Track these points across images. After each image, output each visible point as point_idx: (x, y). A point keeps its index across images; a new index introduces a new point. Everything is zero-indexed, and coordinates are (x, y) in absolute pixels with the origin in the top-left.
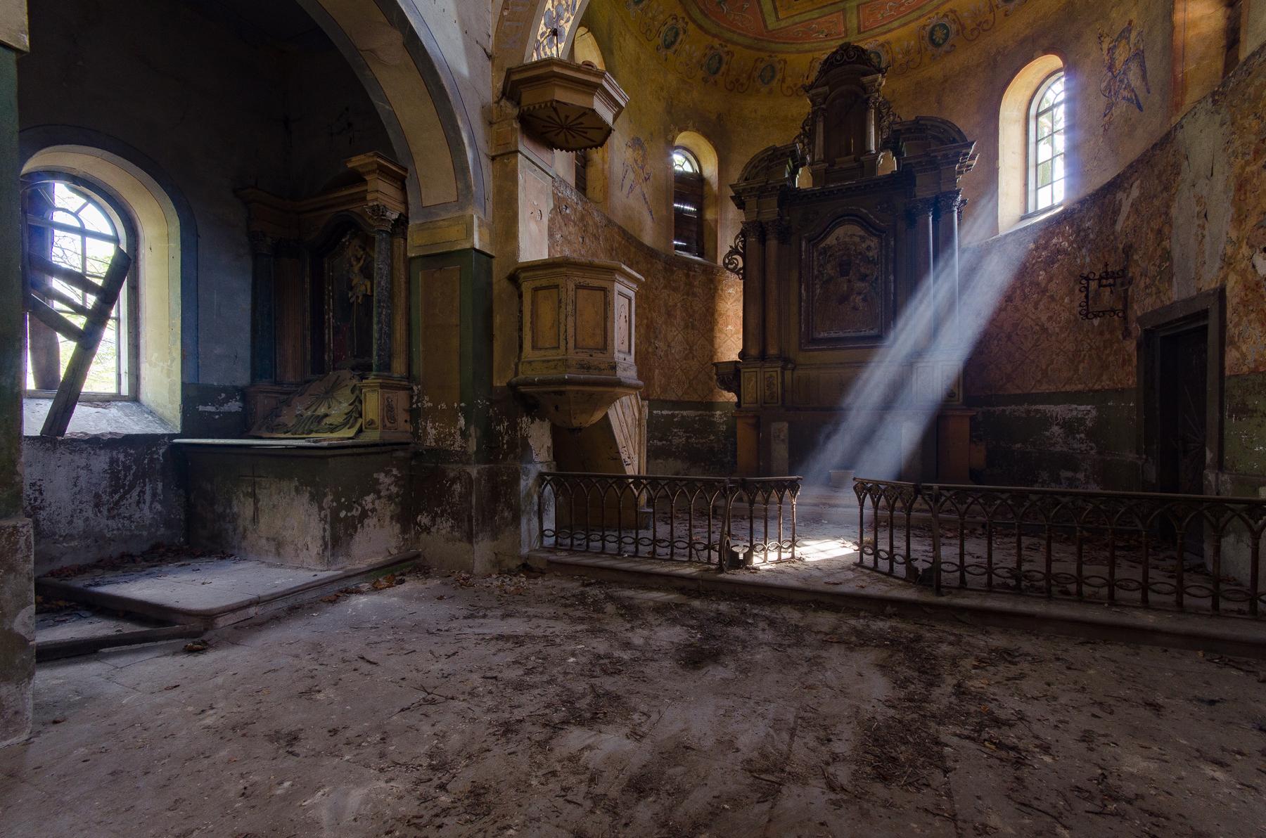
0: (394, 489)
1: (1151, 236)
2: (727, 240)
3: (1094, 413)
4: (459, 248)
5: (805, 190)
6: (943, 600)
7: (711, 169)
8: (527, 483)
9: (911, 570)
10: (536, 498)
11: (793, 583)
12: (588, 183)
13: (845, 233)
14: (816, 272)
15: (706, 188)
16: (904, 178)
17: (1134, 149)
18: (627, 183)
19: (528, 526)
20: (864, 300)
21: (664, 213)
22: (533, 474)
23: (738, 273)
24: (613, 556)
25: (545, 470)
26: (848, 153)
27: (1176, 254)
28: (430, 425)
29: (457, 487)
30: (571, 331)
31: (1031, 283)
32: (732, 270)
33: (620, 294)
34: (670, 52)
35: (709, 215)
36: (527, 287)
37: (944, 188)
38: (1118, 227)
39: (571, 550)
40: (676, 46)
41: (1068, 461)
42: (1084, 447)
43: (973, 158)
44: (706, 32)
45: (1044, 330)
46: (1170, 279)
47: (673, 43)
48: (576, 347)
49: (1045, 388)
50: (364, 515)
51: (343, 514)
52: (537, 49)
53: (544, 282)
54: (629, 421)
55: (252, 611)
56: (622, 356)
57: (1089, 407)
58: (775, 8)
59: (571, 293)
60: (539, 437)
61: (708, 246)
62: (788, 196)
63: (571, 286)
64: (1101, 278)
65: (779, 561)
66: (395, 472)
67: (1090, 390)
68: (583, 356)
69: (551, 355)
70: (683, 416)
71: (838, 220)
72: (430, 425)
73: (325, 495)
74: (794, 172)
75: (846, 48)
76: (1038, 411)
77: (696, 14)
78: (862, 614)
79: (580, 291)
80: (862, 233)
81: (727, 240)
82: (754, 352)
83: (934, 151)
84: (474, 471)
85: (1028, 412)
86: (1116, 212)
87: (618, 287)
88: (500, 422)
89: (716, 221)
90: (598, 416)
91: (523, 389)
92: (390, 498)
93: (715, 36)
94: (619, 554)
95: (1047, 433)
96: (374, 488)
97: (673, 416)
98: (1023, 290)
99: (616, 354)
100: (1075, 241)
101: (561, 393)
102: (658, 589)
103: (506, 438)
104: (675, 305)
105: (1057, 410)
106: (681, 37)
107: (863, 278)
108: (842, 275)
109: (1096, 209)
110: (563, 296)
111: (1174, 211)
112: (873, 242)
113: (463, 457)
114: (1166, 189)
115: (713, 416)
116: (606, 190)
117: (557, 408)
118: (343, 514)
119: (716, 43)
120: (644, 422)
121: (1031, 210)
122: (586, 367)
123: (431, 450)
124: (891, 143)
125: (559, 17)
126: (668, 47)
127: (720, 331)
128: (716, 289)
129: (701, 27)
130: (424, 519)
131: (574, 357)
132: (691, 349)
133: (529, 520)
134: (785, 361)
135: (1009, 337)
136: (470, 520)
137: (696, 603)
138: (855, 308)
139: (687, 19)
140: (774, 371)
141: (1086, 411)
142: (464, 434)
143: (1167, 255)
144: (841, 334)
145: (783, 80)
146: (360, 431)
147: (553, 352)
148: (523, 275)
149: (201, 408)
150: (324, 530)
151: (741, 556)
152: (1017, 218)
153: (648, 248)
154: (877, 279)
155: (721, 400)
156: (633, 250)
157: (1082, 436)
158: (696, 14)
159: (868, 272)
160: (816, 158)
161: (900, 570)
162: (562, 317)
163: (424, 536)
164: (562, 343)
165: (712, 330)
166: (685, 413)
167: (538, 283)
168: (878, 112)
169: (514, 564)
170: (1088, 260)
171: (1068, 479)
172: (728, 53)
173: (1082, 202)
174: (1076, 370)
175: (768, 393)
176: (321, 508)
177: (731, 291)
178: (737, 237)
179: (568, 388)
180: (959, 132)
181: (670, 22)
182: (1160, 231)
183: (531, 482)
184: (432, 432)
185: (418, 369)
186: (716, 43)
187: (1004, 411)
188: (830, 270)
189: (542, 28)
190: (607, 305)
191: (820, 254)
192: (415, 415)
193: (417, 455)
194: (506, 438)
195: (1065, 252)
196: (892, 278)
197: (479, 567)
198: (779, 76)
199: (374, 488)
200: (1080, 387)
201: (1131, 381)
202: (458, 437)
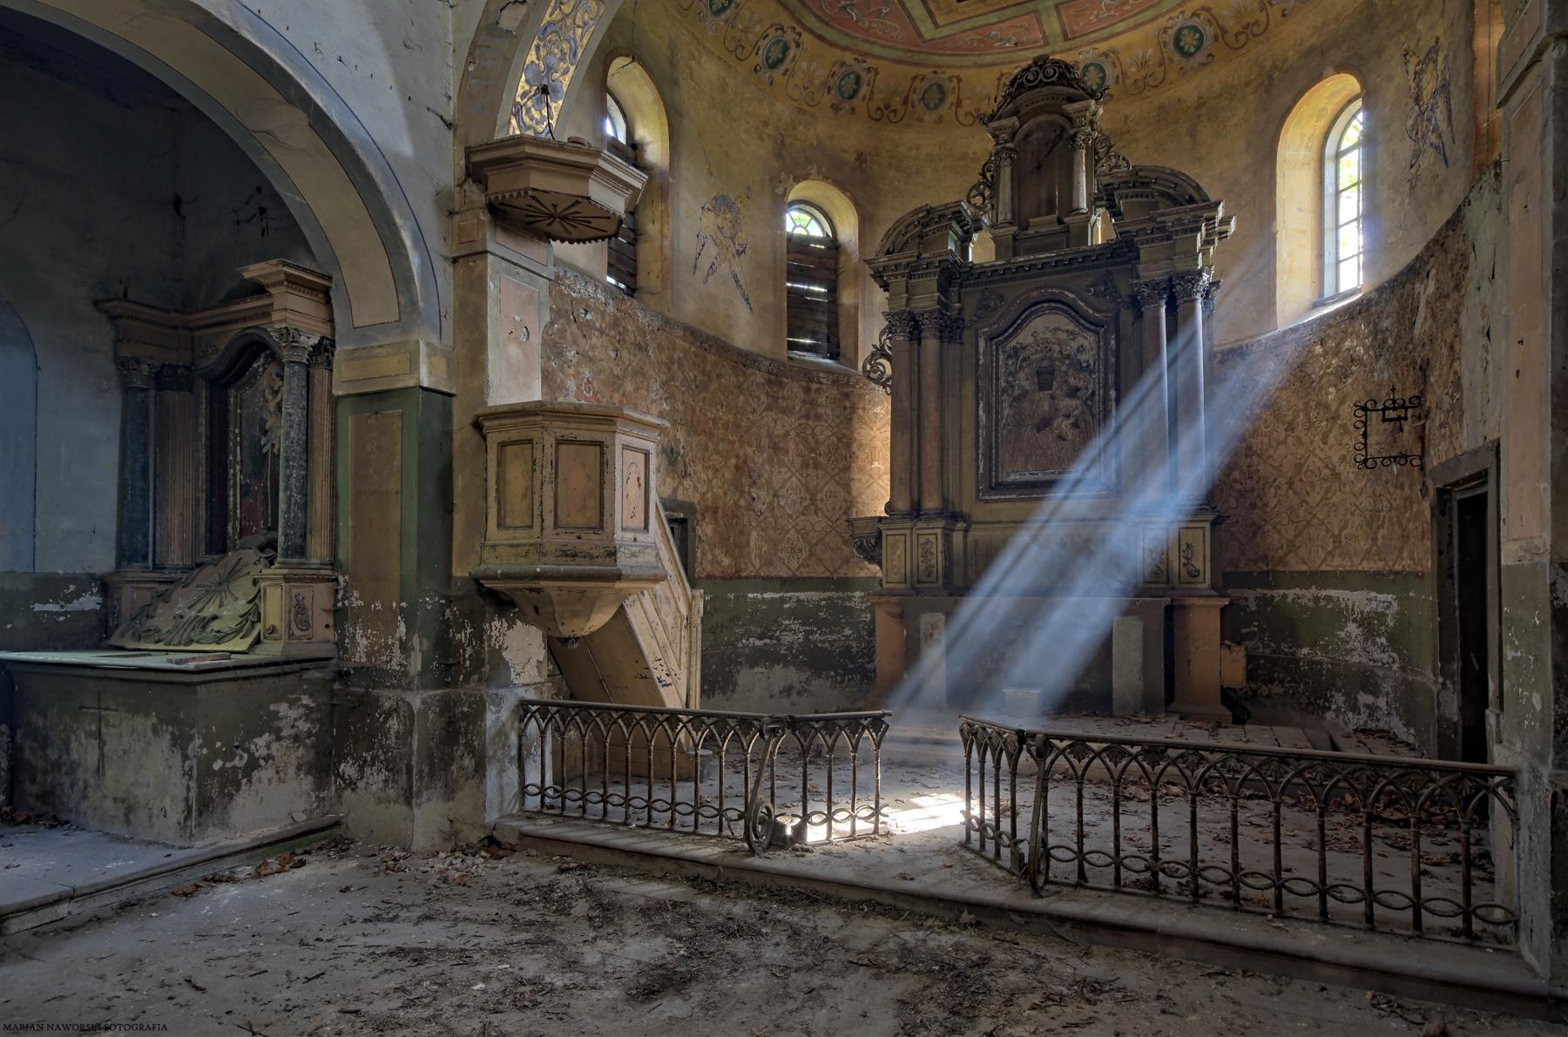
0: (303, 726)
1: (1445, 351)
2: (870, 332)
3: (1395, 606)
4: (400, 385)
5: (981, 266)
6: (1038, 904)
7: (848, 231)
8: (497, 717)
9: (1018, 857)
10: (513, 738)
11: (845, 873)
12: (641, 266)
14: (1003, 384)
15: (842, 259)
16: (1122, 251)
17: (1439, 217)
18: (705, 263)
19: (500, 783)
20: (1075, 425)
21: (771, 299)
22: (510, 699)
24: (615, 826)
25: (531, 695)
26: (1050, 211)
27: (1465, 382)
28: (359, 632)
30: (549, 504)
31: (1318, 404)
32: (877, 381)
33: (626, 447)
34: (777, 74)
35: (847, 298)
36: (493, 439)
37: (1181, 267)
38: (1417, 330)
39: (562, 817)
40: (787, 64)
41: (1367, 680)
42: (1385, 656)
43: (1226, 221)
44: (832, 44)
45: (1336, 475)
46: (1461, 417)
47: (780, 61)
48: (556, 525)
49: (1337, 564)
50: (253, 764)
51: (217, 765)
52: (517, 114)
54: (670, 621)
55: (63, 909)
56: (630, 535)
57: (1390, 597)
58: (930, 12)
59: (550, 451)
60: (522, 650)
61: (845, 342)
62: (954, 275)
63: (550, 440)
64: (1385, 409)
65: (852, 837)
66: (306, 700)
67: (1391, 572)
68: (569, 540)
69: (522, 537)
70: (799, 601)
71: (1032, 308)
72: (359, 632)
73: (191, 738)
74: (964, 241)
75: (1041, 63)
76: (1329, 599)
77: (811, 22)
78: (929, 922)
79: (563, 448)
80: (1071, 327)
81: (870, 332)
82: (903, 505)
83: (1162, 215)
84: (416, 700)
85: (1317, 599)
86: (1414, 311)
87: (620, 439)
88: (461, 628)
89: (856, 308)
90: (599, 619)
91: (488, 584)
92: (296, 738)
93: (845, 49)
94: (625, 824)
95: (1343, 634)
96: (271, 725)
97: (783, 600)
98: (1307, 414)
99: (619, 534)
100: (1371, 346)
101: (539, 590)
102: (662, 879)
103: (469, 651)
104: (787, 434)
105: (1358, 599)
106: (793, 51)
108: (1042, 389)
109: (1395, 302)
110: (538, 454)
111: (1463, 321)
113: (401, 680)
114: (1457, 287)
115: (849, 599)
116: (667, 276)
117: (536, 610)
118: (217, 765)
119: (848, 57)
120: (697, 620)
121: (1328, 293)
123: (360, 669)
124: (1106, 197)
125: (550, 69)
126: (773, 66)
127: (861, 470)
128: (854, 408)
129: (821, 38)
130: (348, 769)
131: (554, 540)
132: (813, 500)
133: (501, 771)
134: (952, 516)
135: (1290, 484)
137: (704, 902)
138: (1061, 437)
139: (798, 29)
140: (932, 534)
141: (1382, 601)
142: (405, 647)
143: (1457, 384)
145: (959, 104)
146: (257, 641)
147: (525, 533)
148: (487, 424)
149: (38, 607)
150: (188, 788)
151: (789, 832)
152: (1307, 304)
153: (740, 353)
154: (1093, 394)
155: (862, 574)
156: (711, 358)
157: (1383, 640)
158: (811, 22)
159: (1081, 384)
160: (1001, 218)
162: (537, 484)
163: (348, 793)
164: (537, 521)
165: (848, 469)
166: (802, 596)
167: (505, 436)
168: (1093, 152)
169: (475, 836)
170: (1386, 375)
171: (1367, 706)
172: (869, 70)
173: (1380, 290)
174: (1375, 539)
175: (923, 567)
176: (185, 757)
177: (878, 410)
178: (882, 333)
179: (543, 584)
180: (1198, 188)
181: (773, 33)
182: (1452, 348)
183: (505, 714)
185: (344, 554)
186: (848, 57)
187: (1285, 596)
188: (1024, 381)
189: (523, 86)
191: (1009, 357)
192: (339, 616)
193: (342, 675)
194: (469, 651)
195: (1361, 363)
196: (1113, 394)
197: (420, 841)
198: (951, 98)
199: (271, 725)
200: (1380, 565)
201: (1428, 564)
202: (396, 650)
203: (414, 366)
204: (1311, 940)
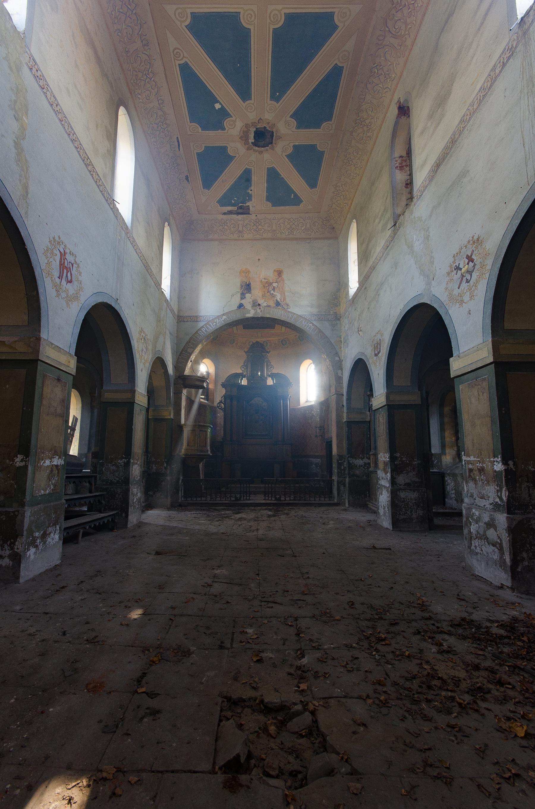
9: (276, 498)
23: (222, 410)
122: (202, 451)
130: (151, 493)
141: (318, 460)
145: (237, 344)
161: (273, 499)
168: (267, 364)
184: (155, 468)
190: (206, 435)
203: (170, 414)
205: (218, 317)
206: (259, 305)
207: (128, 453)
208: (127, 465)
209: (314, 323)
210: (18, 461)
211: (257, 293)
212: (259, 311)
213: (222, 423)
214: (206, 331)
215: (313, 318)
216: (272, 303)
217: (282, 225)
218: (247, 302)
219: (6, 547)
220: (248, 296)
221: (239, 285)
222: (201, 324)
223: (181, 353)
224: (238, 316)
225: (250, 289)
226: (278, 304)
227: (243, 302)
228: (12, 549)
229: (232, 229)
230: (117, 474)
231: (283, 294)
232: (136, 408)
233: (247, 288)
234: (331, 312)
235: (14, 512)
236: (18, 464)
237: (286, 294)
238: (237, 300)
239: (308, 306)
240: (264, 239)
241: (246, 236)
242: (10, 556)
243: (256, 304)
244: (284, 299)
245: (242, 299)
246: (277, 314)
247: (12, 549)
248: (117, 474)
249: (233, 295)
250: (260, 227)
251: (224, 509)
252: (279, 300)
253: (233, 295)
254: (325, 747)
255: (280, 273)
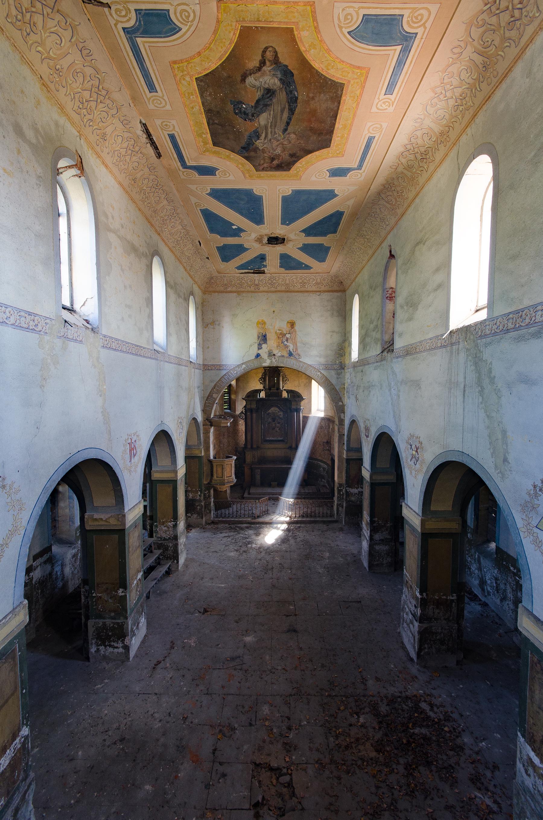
13: (273, 410)
29: (199, 507)
53: (219, 463)
71: (272, 406)
107: (279, 423)
112: (281, 413)
113: (200, 501)
130: (189, 515)
136: (202, 514)
138: (277, 432)
142: (200, 496)
144: (273, 439)
188: (270, 420)
202: (198, 496)
204: (318, 519)
205: (238, 366)
206: (274, 355)
207: (175, 518)
208: (175, 526)
209: (322, 371)
210: (120, 592)
211: (272, 343)
212: (274, 360)
213: (244, 429)
214: (228, 378)
215: (321, 368)
216: (285, 354)
217: (295, 280)
218: (264, 353)
219: (119, 642)
220: (264, 346)
221: (256, 336)
222: (224, 372)
223: (208, 398)
224: (256, 364)
225: (266, 339)
226: (291, 354)
227: (260, 352)
228: (123, 643)
229: (249, 283)
230: (168, 533)
231: (295, 344)
232: (179, 482)
233: (263, 338)
234: (337, 361)
235: (122, 623)
236: (120, 594)
237: (298, 344)
238: (254, 350)
239: (317, 356)
240: (279, 291)
241: (262, 289)
242: (122, 647)
243: (271, 355)
244: (297, 349)
245: (259, 349)
246: (290, 363)
247: (123, 643)
248: (168, 533)
249: (251, 346)
250: (274, 281)
251: (247, 528)
252: (291, 350)
253: (251, 346)
254: (293, 794)
255: (292, 324)
